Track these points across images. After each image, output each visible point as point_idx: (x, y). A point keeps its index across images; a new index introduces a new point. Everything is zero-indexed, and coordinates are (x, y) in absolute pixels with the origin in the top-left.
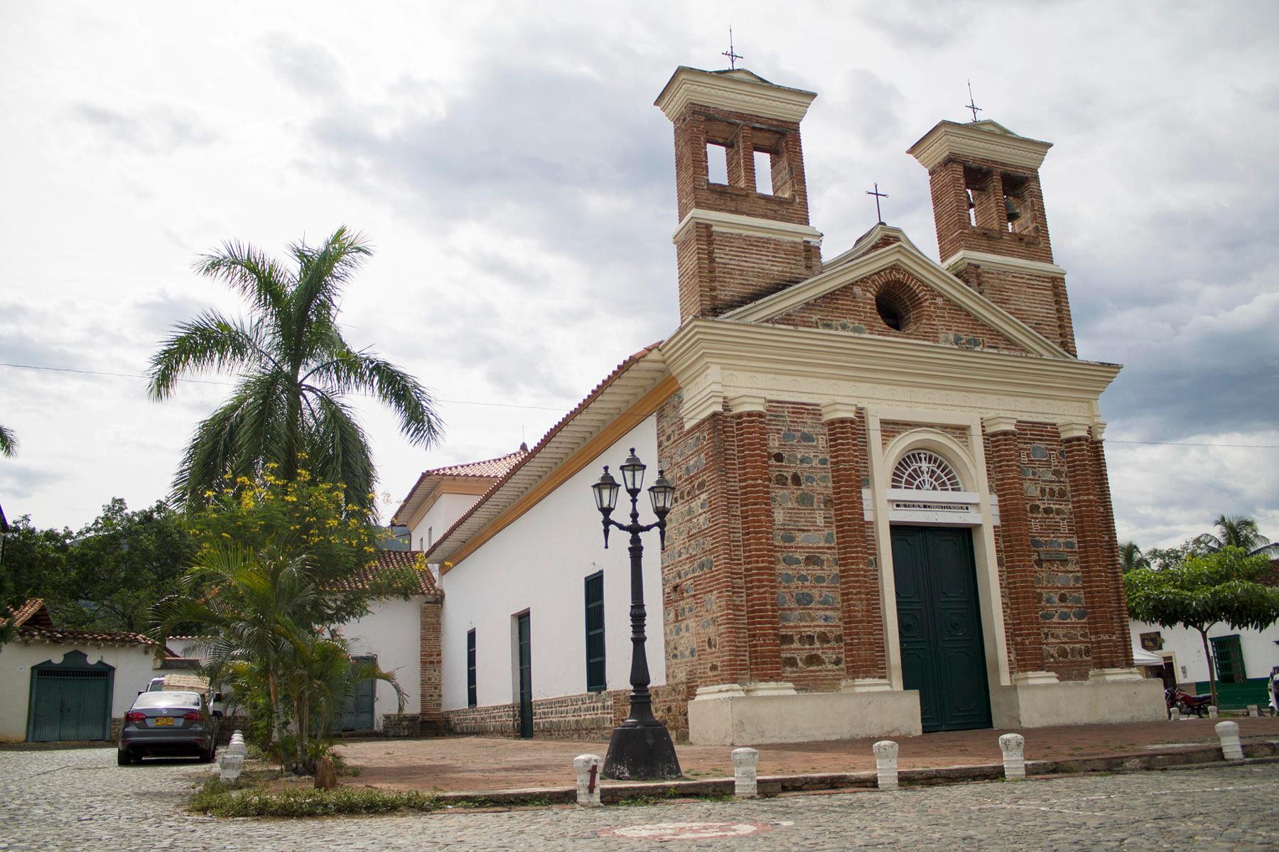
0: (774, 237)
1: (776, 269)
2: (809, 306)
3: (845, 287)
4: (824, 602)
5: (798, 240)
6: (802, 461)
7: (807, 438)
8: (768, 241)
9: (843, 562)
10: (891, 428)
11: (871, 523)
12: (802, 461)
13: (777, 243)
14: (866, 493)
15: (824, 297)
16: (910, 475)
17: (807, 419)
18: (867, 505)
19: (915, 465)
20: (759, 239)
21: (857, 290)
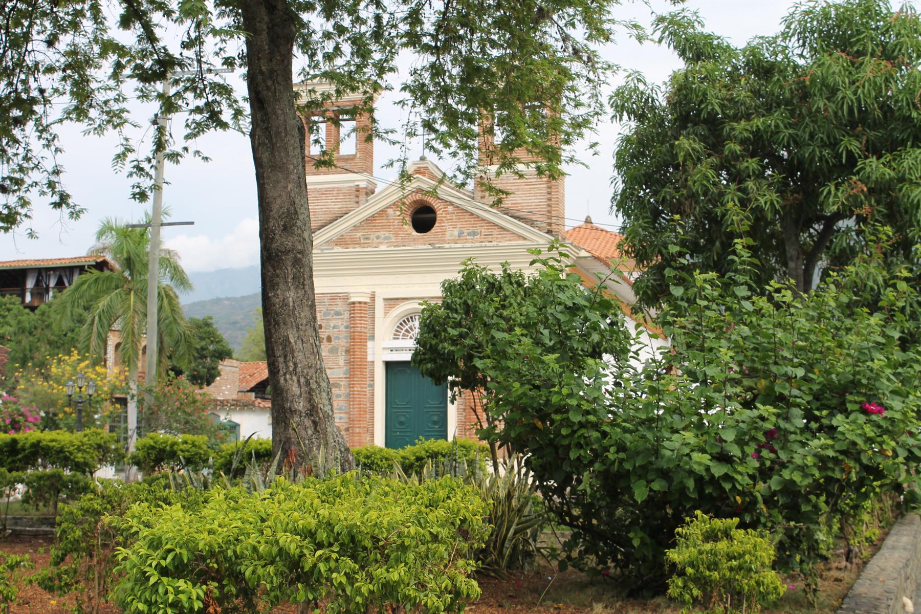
0: (336, 185)
1: (336, 207)
2: (356, 228)
3: (382, 211)
4: (340, 409)
5: (352, 185)
6: (334, 328)
7: (338, 313)
8: (333, 189)
9: (351, 386)
10: (392, 302)
11: (373, 362)
12: (334, 328)
13: (339, 189)
14: (370, 344)
15: (367, 220)
16: (406, 330)
17: (339, 302)
18: (369, 351)
19: (411, 324)
20: (327, 190)
21: (390, 211)
